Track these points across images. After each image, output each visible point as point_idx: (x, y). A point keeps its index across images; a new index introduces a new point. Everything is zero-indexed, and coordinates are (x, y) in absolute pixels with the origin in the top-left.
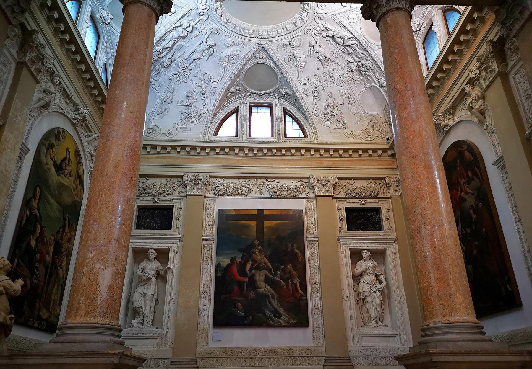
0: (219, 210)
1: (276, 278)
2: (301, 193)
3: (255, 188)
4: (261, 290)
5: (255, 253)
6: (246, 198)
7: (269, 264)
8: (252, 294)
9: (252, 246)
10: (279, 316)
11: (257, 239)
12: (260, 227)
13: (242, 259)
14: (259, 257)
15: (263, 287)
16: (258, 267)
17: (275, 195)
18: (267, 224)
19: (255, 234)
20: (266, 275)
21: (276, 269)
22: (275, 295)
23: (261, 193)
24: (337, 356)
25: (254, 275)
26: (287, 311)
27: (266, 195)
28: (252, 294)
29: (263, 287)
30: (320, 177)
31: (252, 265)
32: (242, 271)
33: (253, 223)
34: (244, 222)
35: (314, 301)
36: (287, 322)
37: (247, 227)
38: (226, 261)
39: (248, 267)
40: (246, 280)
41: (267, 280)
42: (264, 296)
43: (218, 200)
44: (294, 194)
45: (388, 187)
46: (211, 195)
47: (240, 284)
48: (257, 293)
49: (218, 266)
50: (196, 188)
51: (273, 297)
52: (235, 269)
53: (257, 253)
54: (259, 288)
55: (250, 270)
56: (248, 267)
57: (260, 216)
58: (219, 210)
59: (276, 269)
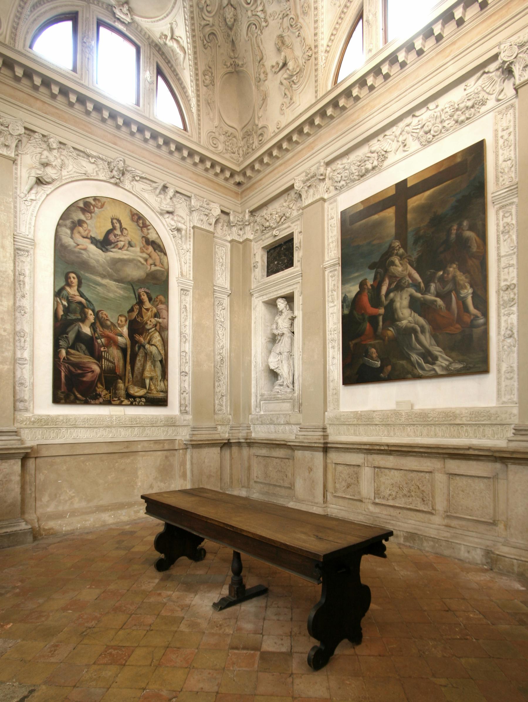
1: (430, 297)
4: (404, 322)
5: (393, 263)
7: (417, 276)
8: (391, 332)
13: (375, 279)
14: (400, 269)
15: (407, 316)
22: (427, 327)
25: (392, 301)
26: (449, 349)
28: (391, 332)
31: (390, 285)
38: (354, 289)
40: (382, 311)
41: (415, 305)
47: (374, 320)
48: (399, 330)
51: (423, 331)
52: (365, 299)
53: (397, 262)
54: (400, 320)
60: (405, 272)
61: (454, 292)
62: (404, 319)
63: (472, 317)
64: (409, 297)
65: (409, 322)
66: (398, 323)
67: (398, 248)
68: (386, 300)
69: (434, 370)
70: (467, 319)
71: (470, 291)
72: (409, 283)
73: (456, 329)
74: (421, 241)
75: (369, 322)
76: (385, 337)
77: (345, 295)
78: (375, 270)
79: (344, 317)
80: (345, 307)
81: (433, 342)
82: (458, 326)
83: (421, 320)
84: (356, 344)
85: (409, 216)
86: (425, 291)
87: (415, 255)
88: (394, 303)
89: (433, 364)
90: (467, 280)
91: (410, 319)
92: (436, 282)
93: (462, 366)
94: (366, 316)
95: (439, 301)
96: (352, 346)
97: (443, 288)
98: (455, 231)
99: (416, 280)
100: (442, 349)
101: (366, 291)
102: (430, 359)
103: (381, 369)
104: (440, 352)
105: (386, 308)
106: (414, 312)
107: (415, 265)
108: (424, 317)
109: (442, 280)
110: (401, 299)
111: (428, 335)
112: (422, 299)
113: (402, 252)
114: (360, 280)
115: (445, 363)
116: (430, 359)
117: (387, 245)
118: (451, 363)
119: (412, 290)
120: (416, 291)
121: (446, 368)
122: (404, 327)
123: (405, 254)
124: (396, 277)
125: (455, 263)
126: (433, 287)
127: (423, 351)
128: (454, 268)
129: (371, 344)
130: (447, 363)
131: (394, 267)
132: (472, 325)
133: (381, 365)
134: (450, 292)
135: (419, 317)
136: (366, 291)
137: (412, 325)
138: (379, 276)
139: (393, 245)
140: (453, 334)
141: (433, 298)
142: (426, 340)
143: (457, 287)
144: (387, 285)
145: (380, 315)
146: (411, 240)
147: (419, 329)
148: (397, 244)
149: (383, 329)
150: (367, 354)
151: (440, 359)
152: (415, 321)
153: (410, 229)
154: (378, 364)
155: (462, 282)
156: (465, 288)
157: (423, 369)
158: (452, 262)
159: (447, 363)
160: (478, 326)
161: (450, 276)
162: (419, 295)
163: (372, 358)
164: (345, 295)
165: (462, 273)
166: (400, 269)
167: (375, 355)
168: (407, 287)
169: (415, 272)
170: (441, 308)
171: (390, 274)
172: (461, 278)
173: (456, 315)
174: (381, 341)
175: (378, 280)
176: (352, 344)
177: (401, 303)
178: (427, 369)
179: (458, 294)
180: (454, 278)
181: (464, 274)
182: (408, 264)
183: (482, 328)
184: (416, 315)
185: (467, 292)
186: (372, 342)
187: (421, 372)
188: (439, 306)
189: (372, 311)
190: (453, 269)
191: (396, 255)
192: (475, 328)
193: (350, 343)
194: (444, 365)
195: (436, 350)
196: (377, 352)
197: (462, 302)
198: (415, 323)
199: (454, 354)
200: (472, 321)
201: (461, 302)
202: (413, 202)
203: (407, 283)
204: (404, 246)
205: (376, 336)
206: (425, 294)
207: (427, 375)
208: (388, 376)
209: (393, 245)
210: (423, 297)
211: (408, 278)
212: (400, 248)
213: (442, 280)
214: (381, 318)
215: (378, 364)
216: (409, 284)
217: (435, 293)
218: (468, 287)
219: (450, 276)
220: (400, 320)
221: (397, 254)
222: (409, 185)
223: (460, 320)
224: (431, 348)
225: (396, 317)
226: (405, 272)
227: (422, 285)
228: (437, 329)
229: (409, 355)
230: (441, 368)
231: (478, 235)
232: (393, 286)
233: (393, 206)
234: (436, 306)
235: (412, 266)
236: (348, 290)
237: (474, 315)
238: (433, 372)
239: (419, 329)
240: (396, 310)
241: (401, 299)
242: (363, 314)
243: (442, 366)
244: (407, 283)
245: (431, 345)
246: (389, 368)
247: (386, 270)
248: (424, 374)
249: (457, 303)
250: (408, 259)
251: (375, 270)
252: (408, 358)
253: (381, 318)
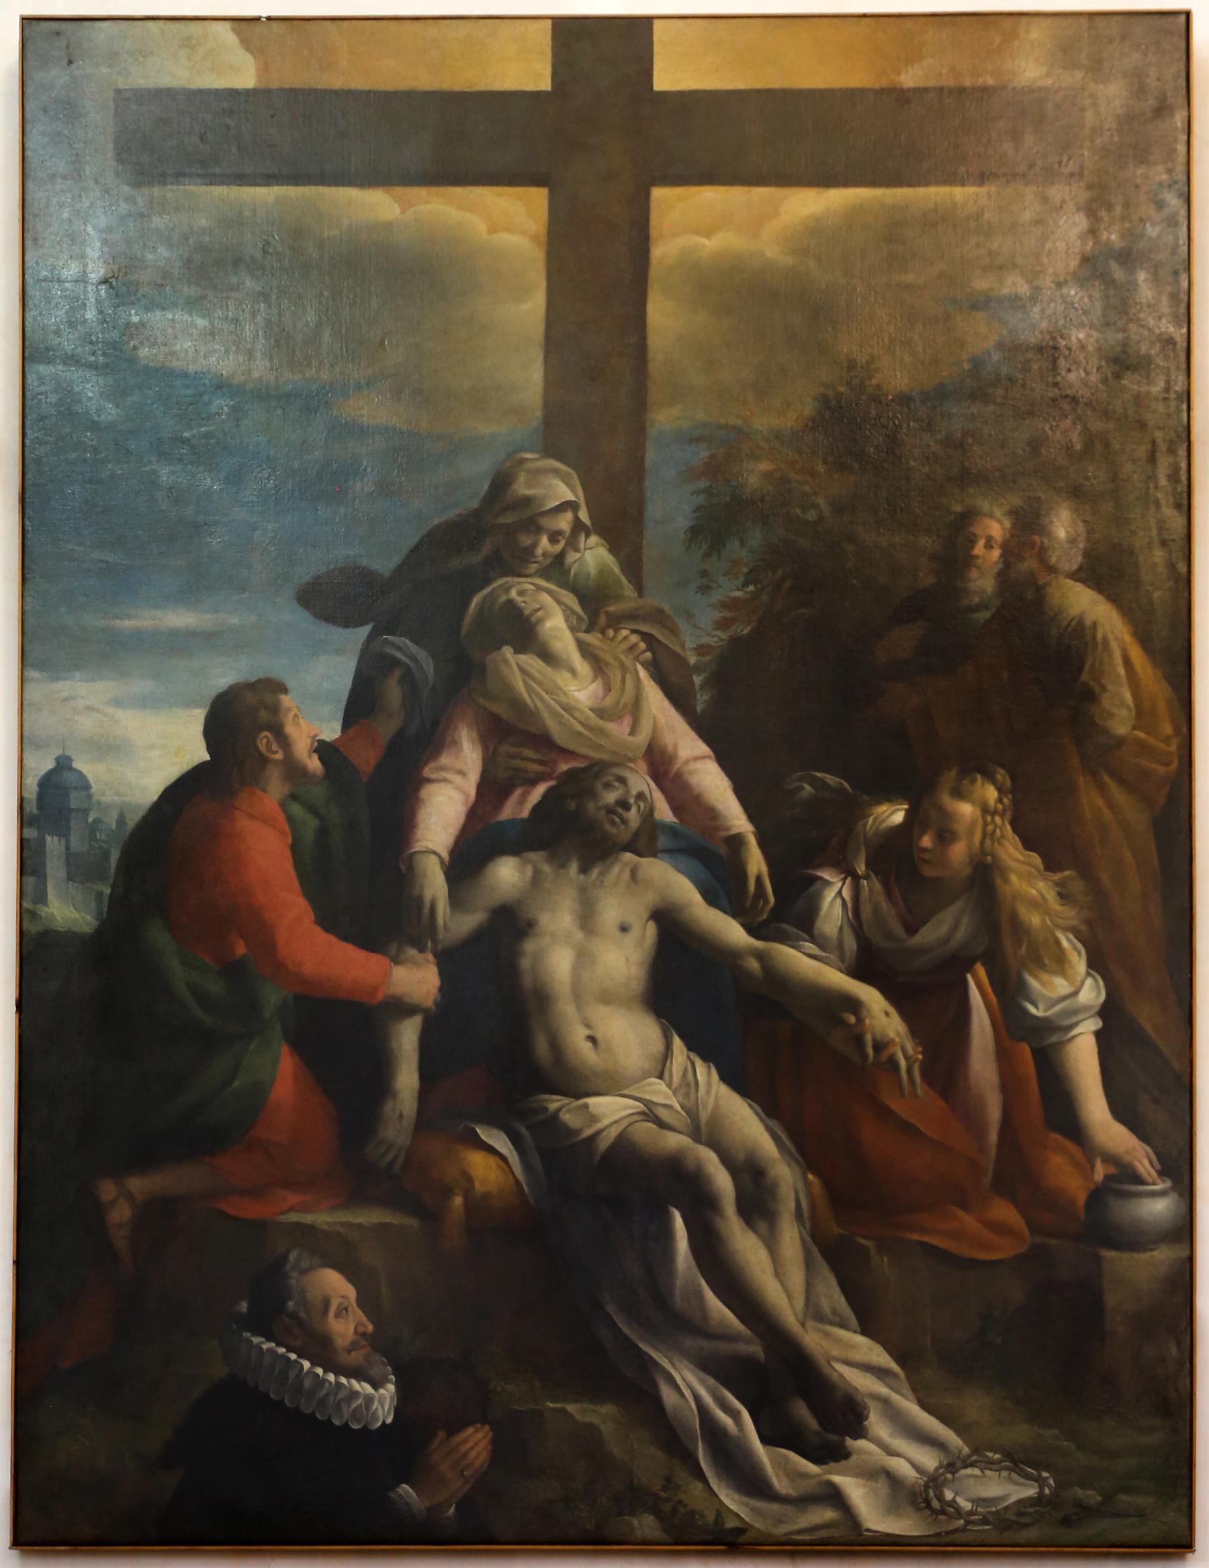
1: (802, 962)
4: (609, 1112)
5: (522, 632)
7: (713, 782)
8: (492, 1163)
11: (561, 432)
12: (600, 269)
13: (360, 705)
14: (581, 690)
15: (633, 1074)
16: (566, 815)
19: (527, 377)
20: (668, 921)
21: (804, 843)
22: (785, 1175)
25: (510, 925)
28: (492, 1163)
29: (633, 1074)
31: (492, 790)
32: (362, 875)
33: (504, 223)
34: (376, 206)
37: (418, 277)
38: (149, 748)
40: (418, 979)
41: (686, 986)
42: (640, 1185)
47: (342, 1037)
51: (757, 1203)
53: (556, 626)
54: (577, 1085)
55: (468, 859)
59: (804, 843)
60: (619, 730)
61: (981, 970)
62: (612, 1084)
63: (1100, 1172)
64: (652, 929)
65: (650, 1114)
66: (555, 1103)
67: (564, 523)
68: (457, 900)
69: (835, 1497)
70: (1067, 1178)
71: (1091, 993)
72: (648, 815)
73: (992, 1229)
74: (756, 538)
75: (299, 1045)
76: (447, 1192)
77: (63, 764)
78: (364, 631)
79: (36, 950)
80: (55, 869)
81: (832, 1295)
82: (1005, 1212)
83: (747, 1123)
84: (157, 1215)
85: (664, 317)
86: (777, 914)
87: (699, 634)
88: (529, 946)
89: (829, 1452)
90: (1070, 915)
91: (659, 1092)
92: (861, 868)
93: (1031, 1491)
94: (272, 997)
95: (881, 1015)
96: (121, 1214)
97: (912, 930)
98: (996, 553)
99: (712, 814)
100: (900, 1359)
101: (275, 788)
102: (802, 1411)
103: (404, 1445)
104: (881, 1373)
105: (448, 960)
106: (691, 1046)
107: (702, 701)
108: (769, 1107)
109: (896, 859)
110: (587, 919)
111: (790, 1237)
112: (754, 965)
113: (603, 571)
114: (224, 675)
115: (913, 1460)
116: (802, 1411)
117: (477, 471)
118: (951, 1467)
119: (682, 888)
120: (710, 898)
122: (604, 1144)
123: (628, 590)
124: (543, 741)
125: (990, 777)
126: (833, 899)
127: (756, 1349)
128: (985, 810)
129: (311, 1229)
130: (929, 1460)
131: (531, 661)
132: (1099, 1224)
133: (398, 1411)
134: (955, 966)
135: (724, 1089)
136: (275, 788)
137: (675, 1141)
138: (393, 693)
139: (522, 487)
140: (975, 1263)
141: (836, 978)
142: (778, 1268)
143: (1002, 950)
144: (470, 783)
145: (401, 1008)
146: (670, 508)
147: (723, 1181)
148: (559, 488)
149: (424, 1122)
150: (274, 1307)
151: (877, 1424)
152: (692, 1113)
153: (665, 419)
154: (381, 1401)
155: (1034, 920)
156: (1060, 963)
157: (752, 1483)
158: (976, 765)
159: (929, 1460)
160: (1135, 1240)
161: (959, 851)
162: (733, 932)
163: (321, 1348)
164: (63, 764)
165: (1036, 859)
166: (581, 690)
167: (345, 1327)
168: (631, 847)
169: (704, 749)
170: (893, 1063)
171: (502, 710)
172: (1029, 885)
173: (993, 1137)
174: (410, 1222)
175: (386, 728)
176: (121, 1200)
177: (583, 958)
178: (780, 1484)
179: (1009, 995)
180: (984, 876)
181: (1051, 865)
182: (643, 673)
183: (1163, 1255)
184: (705, 1074)
185: (1070, 991)
186: (322, 1218)
187: (730, 1499)
188: (879, 1046)
189: (326, 957)
190: (974, 809)
191: (545, 573)
192: (1118, 1246)
193: (107, 1190)
194: (902, 1468)
195: (854, 1358)
196: (367, 1301)
197: (1034, 1046)
198: (696, 1134)
199: (977, 1404)
200: (1097, 1197)
201: (1025, 1050)
202: (699, 224)
203: (633, 816)
204: (619, 520)
205: (357, 1169)
206: (782, 938)
207: (780, 1530)
208: (464, 1504)
209: (522, 487)
210: (760, 956)
211: (640, 781)
212: (578, 526)
213: (896, 859)
214: (407, 1038)
215: (381, 1401)
216: (650, 824)
217: (851, 944)
218: (1080, 964)
219: (959, 851)
220: (577, 1085)
221: (556, 569)
222: (668, 76)
223: (1016, 1175)
224: (812, 1339)
225: (542, 1049)
226: (619, 730)
227: (756, 862)
229: (647, 1366)
230: (882, 1486)
231: (1144, 639)
232: (521, 805)
233: (536, 180)
234: (859, 1040)
235: (679, 698)
236: (87, 725)
237: (1110, 1158)
238: (829, 1514)
239: (723, 1181)
240: (542, 998)
241: (587, 919)
242: (234, 972)
243: (893, 1479)
244: (633, 816)
245: (814, 1313)
246: (475, 1443)
247: (464, 674)
248: (758, 1524)
249: (1003, 1055)
250: (646, 637)
251: (364, 631)
252: (640, 1394)
253: (407, 1038)
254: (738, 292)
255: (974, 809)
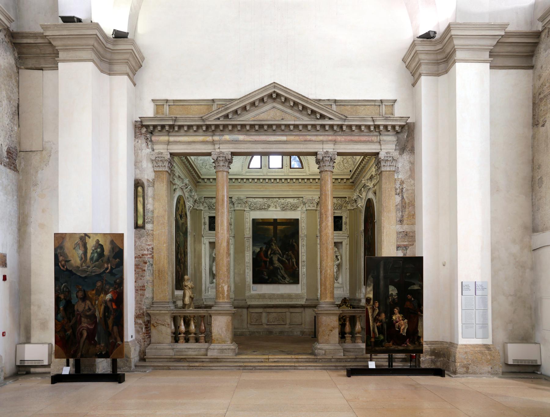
0: (253, 219)
1: (283, 259)
2: (298, 207)
3: (272, 204)
6: (267, 211)
8: (271, 267)
9: (271, 241)
10: (285, 278)
12: (275, 229)
15: (277, 264)
16: (274, 253)
17: (284, 209)
18: (279, 227)
19: (272, 234)
23: (276, 207)
24: (311, 298)
25: (272, 257)
26: (289, 276)
27: (279, 209)
28: (271, 267)
29: (277, 264)
30: (310, 197)
32: (266, 256)
33: (271, 227)
35: (303, 270)
36: (288, 281)
37: (268, 230)
38: (258, 250)
39: (269, 253)
40: (268, 260)
41: (279, 260)
42: (277, 268)
43: (252, 213)
44: (294, 208)
45: (348, 203)
46: (248, 209)
47: (265, 262)
49: (253, 252)
50: (240, 205)
55: (270, 254)
56: (269, 253)
57: (275, 222)
58: (253, 219)
83: (281, 266)
85: (278, 231)
109: (287, 255)
121: (288, 281)
126: (285, 256)
142: (283, 272)
143: (292, 258)
185: (294, 260)
189: (265, 259)
195: (286, 276)
197: (293, 262)
204: (276, 240)
215: (267, 277)
228: (286, 269)
254: (281, 230)
255: (290, 252)
